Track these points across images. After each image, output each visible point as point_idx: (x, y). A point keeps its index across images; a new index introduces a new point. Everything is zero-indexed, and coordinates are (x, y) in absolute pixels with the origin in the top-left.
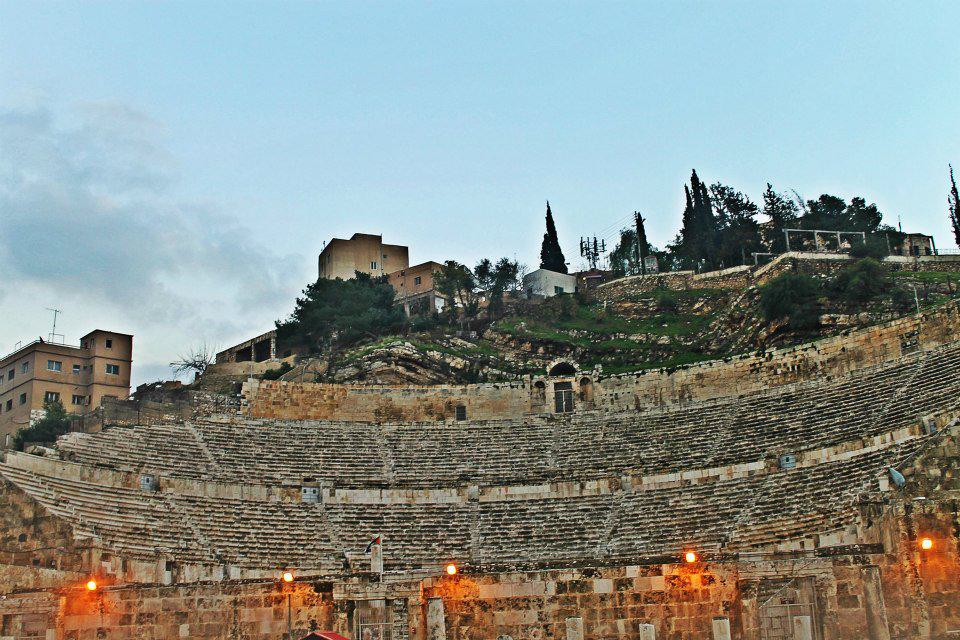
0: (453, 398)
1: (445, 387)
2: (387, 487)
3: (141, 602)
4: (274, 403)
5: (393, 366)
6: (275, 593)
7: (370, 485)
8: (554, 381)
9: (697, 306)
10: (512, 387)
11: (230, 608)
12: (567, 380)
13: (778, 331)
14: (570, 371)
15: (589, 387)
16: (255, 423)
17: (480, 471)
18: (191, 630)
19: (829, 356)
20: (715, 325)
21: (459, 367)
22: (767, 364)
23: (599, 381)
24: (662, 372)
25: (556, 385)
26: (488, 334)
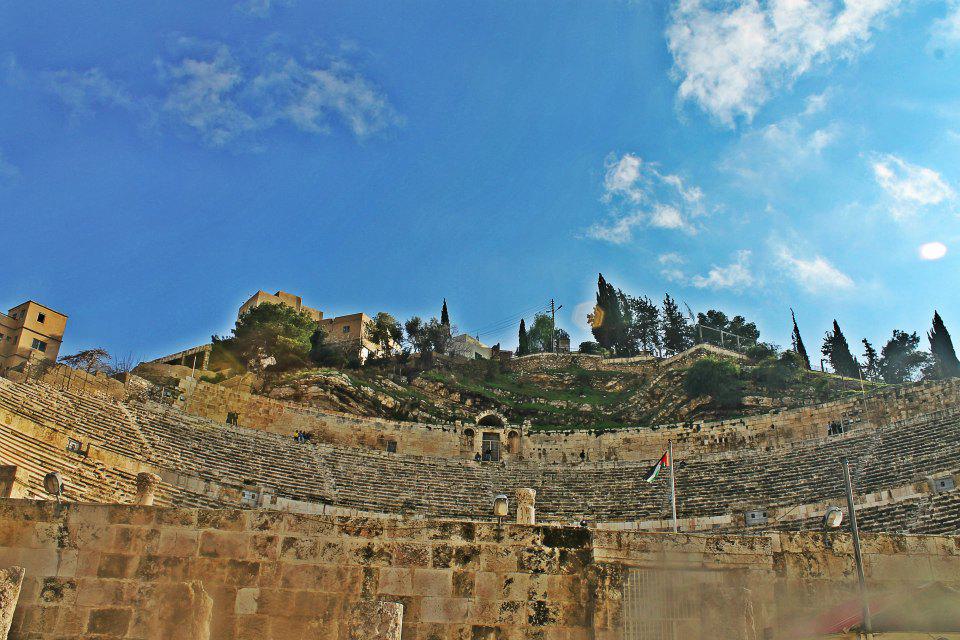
0: (386, 433)
1: (379, 420)
2: (330, 503)
3: (155, 532)
4: (209, 407)
5: (328, 393)
6: (457, 541)
7: (313, 498)
8: (483, 430)
9: (610, 384)
10: (444, 430)
11: (357, 563)
12: (497, 431)
13: (699, 408)
14: (499, 424)
15: (516, 441)
16: (192, 419)
17: (423, 501)
18: (261, 601)
19: (754, 433)
20: (635, 400)
21: (390, 406)
22: (694, 435)
23: (529, 435)
24: (590, 433)
25: (484, 434)
26: (418, 381)
